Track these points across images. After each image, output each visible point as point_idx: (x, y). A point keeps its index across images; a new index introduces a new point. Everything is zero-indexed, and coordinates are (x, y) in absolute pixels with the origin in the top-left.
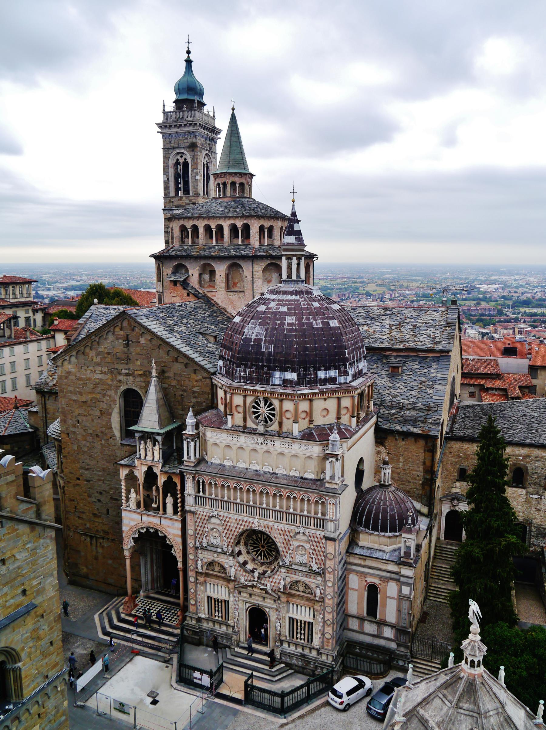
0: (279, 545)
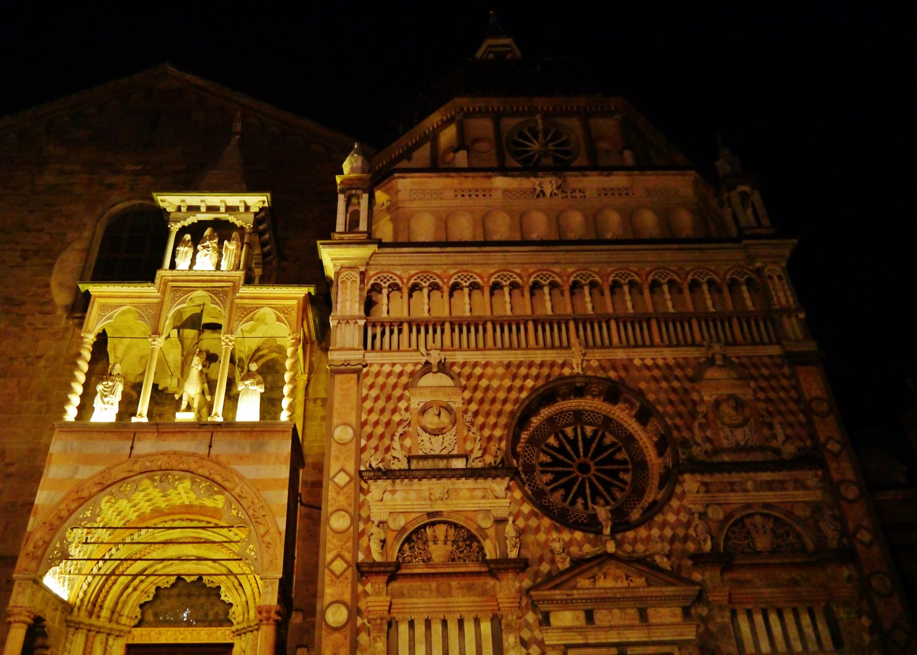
0: (660, 409)
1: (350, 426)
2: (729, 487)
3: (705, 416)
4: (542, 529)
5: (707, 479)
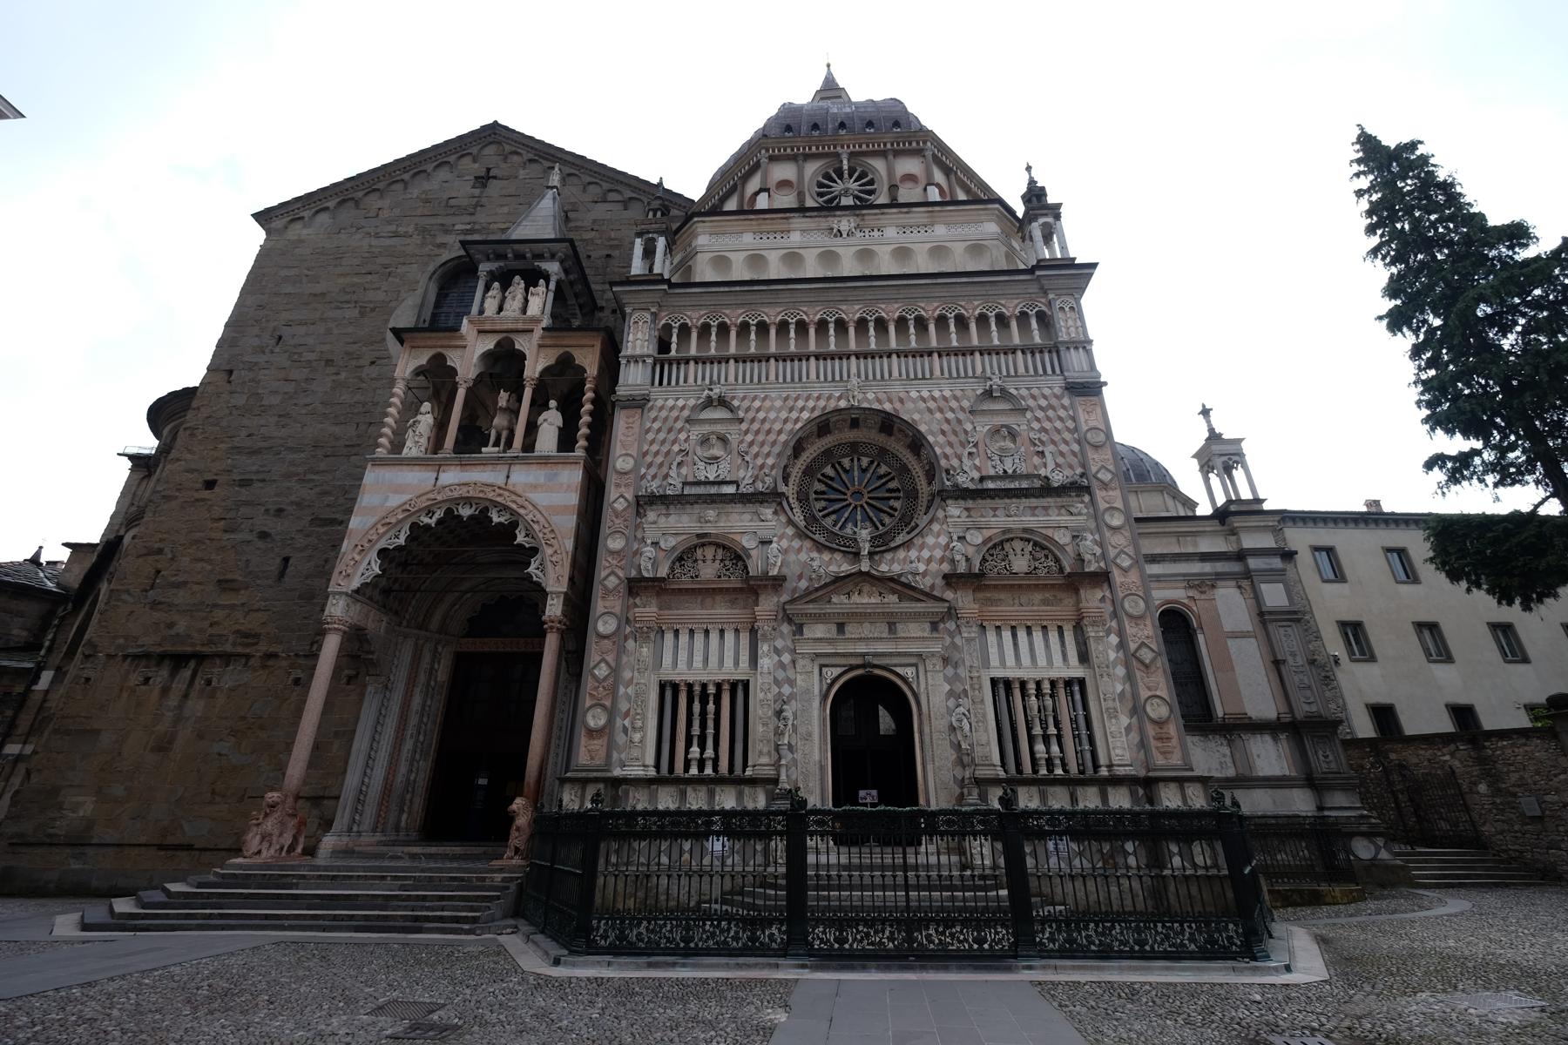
0: (931, 439)
1: (632, 456)
2: (992, 513)
3: (976, 445)
4: (804, 550)
5: (970, 503)
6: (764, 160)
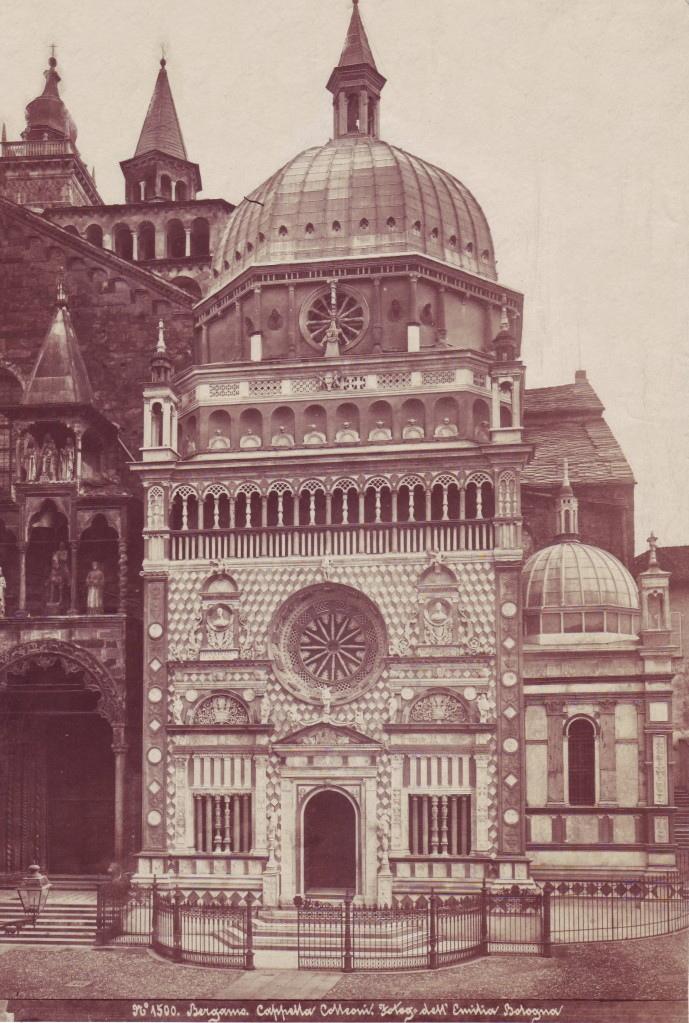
0: (383, 611)
6: (257, 291)
